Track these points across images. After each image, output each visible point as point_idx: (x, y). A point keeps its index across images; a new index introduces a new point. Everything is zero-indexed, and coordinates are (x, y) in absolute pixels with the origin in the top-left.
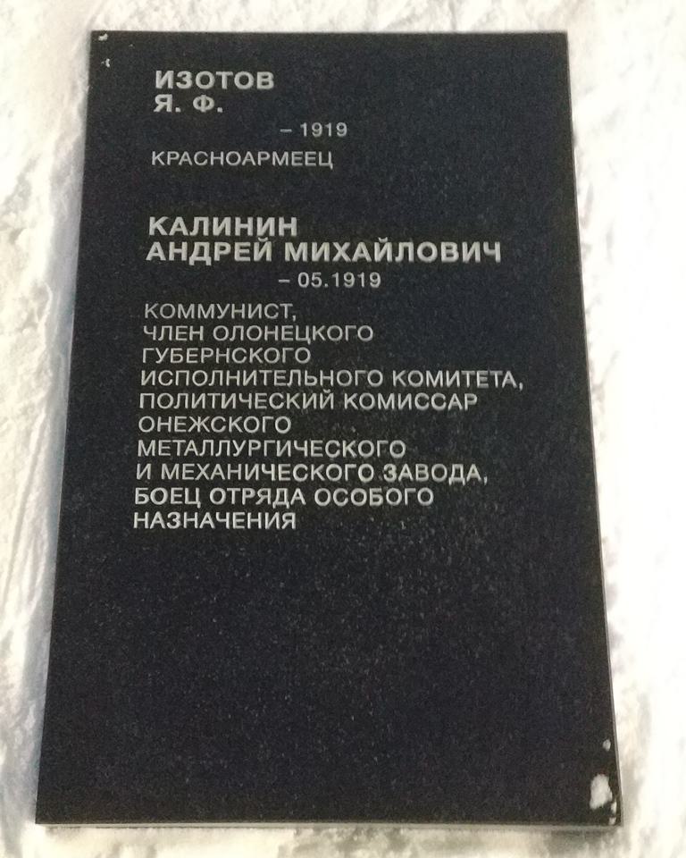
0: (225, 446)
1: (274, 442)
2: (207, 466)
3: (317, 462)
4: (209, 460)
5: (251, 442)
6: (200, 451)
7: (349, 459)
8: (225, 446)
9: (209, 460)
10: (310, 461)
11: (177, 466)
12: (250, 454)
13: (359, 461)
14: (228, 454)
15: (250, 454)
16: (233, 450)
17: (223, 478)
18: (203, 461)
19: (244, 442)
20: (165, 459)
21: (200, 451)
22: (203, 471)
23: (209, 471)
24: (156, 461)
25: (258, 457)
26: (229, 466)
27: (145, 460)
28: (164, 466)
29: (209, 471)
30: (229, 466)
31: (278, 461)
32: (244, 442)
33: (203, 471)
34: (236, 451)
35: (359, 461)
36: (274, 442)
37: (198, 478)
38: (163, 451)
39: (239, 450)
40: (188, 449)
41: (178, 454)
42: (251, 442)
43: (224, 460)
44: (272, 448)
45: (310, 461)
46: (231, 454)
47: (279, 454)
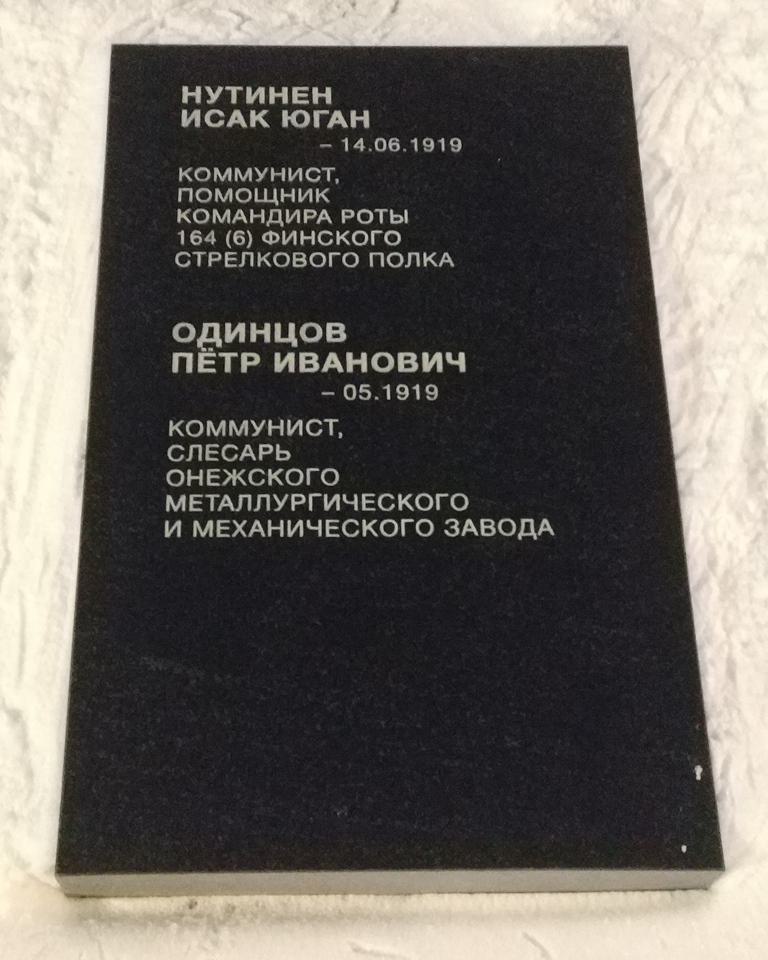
0: (264, 501)
1: (319, 495)
2: (245, 522)
3: (368, 516)
4: (248, 516)
5: (293, 496)
6: (236, 506)
7: (406, 513)
8: (264, 501)
9: (248, 516)
10: (362, 515)
11: (210, 524)
12: (293, 509)
13: (417, 515)
14: (268, 508)
15: (293, 509)
16: (274, 504)
17: (263, 535)
18: (239, 517)
19: (286, 496)
20: (196, 516)
21: (236, 506)
22: (240, 528)
23: (247, 529)
24: (187, 518)
26: (270, 522)
27: (173, 516)
28: (196, 524)
29: (247, 529)
30: (270, 522)
33: (240, 528)
34: (277, 506)
35: (417, 515)
36: (319, 495)
37: (234, 535)
38: (195, 506)
39: (281, 504)
40: (222, 504)
41: (212, 509)
43: (263, 516)
44: (318, 502)
45: (362, 515)
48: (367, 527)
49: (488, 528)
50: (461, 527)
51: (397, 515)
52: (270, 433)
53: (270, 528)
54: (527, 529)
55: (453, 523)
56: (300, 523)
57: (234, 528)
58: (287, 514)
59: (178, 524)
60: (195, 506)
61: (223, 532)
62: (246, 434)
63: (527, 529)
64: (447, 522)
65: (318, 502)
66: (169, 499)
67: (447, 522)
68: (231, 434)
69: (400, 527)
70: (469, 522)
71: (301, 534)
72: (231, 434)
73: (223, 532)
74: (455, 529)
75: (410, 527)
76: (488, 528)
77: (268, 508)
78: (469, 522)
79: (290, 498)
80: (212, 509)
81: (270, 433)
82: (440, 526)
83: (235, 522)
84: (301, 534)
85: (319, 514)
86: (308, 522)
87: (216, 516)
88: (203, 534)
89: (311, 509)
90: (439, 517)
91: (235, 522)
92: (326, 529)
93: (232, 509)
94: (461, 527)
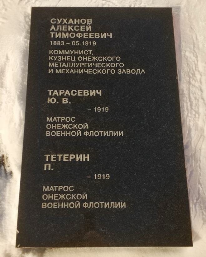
2: (69, 70)
3: (99, 69)
4: (69, 68)
5: (81, 63)
7: (108, 68)
9: (69, 68)
11: (60, 70)
13: (111, 68)
14: (75, 66)
16: (76, 65)
17: (73, 73)
18: (67, 68)
19: (79, 63)
22: (67, 71)
23: (69, 71)
24: (54, 68)
25: (83, 68)
27: (51, 68)
28: (57, 70)
29: (69, 71)
31: (88, 68)
32: (79, 63)
33: (67, 71)
35: (111, 68)
39: (78, 65)
40: (63, 65)
41: (61, 66)
42: (81, 63)
43: (73, 68)
44: (87, 65)
45: (97, 68)
46: (75, 66)
47: (89, 66)
48: (99, 71)
49: (129, 71)
50: (122, 71)
51: (106, 68)
52: (75, 54)
53: (75, 71)
54: (138, 72)
55: (120, 71)
56: (82, 70)
57: (66, 71)
58: (79, 68)
59: (52, 70)
60: (56, 65)
61: (63, 72)
62: (69, 54)
63: (138, 72)
64: (118, 70)
65: (87, 65)
66: (50, 63)
67: (118, 70)
68: (65, 54)
69: (107, 72)
70: (124, 70)
71: (83, 73)
72: (65, 54)
73: (63, 72)
74: (120, 72)
75: (109, 71)
76: (129, 71)
77: (75, 66)
78: (124, 70)
79: (80, 64)
80: (61, 66)
81: (75, 54)
82: (117, 71)
83: (66, 70)
84: (83, 73)
85: (87, 68)
86: (84, 70)
87: (61, 68)
88: (58, 73)
89: (85, 67)
90: (116, 69)
91: (66, 70)
92: (88, 72)
93: (66, 66)
94: (122, 71)
